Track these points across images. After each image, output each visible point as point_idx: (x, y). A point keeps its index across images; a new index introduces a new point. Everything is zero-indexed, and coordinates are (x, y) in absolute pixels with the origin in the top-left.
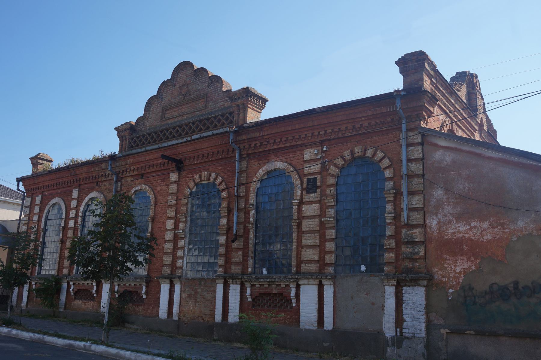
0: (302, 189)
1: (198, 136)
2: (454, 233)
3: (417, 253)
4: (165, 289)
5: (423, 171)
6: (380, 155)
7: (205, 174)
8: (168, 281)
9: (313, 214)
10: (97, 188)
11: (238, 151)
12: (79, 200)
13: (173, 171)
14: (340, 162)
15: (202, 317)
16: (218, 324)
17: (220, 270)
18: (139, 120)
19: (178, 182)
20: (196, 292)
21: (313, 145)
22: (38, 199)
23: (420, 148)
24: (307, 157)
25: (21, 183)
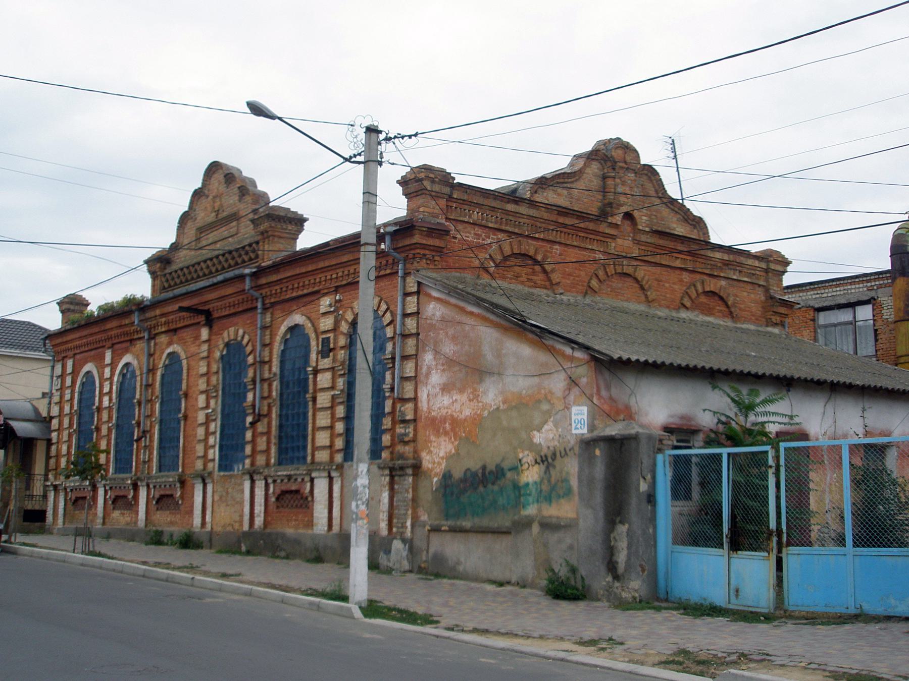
0: (317, 354)
2: (440, 408)
3: (406, 435)
5: (418, 328)
7: (232, 330)
8: (200, 480)
9: (326, 386)
11: (260, 300)
12: (113, 365)
19: (208, 341)
20: (227, 493)
23: (415, 299)
24: (323, 310)
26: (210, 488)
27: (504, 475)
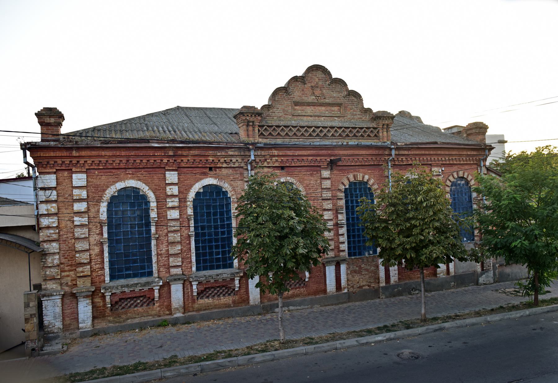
4: (330, 271)
10: (211, 173)
13: (325, 169)
18: (264, 107)
20: (360, 267)
21: (437, 166)
25: (28, 153)
26: (343, 267)
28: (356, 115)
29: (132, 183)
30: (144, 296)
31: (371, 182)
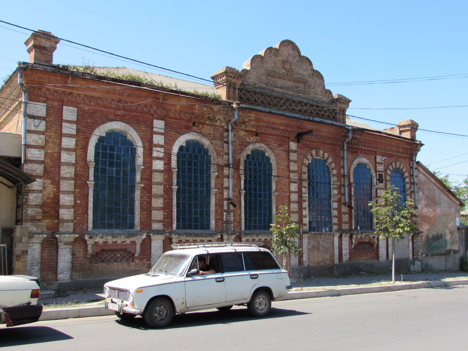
1: (320, 120)
6: (394, 165)
10: (195, 128)
14: (404, 170)
15: (324, 262)
16: (337, 265)
17: (335, 227)
20: (319, 244)
22: (69, 113)
27: (442, 237)
28: (317, 94)
29: (117, 126)
30: (125, 250)
31: (330, 160)
